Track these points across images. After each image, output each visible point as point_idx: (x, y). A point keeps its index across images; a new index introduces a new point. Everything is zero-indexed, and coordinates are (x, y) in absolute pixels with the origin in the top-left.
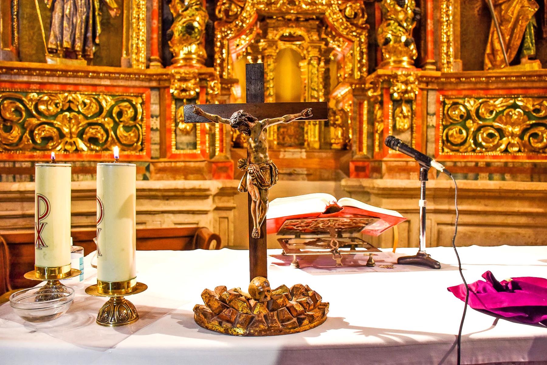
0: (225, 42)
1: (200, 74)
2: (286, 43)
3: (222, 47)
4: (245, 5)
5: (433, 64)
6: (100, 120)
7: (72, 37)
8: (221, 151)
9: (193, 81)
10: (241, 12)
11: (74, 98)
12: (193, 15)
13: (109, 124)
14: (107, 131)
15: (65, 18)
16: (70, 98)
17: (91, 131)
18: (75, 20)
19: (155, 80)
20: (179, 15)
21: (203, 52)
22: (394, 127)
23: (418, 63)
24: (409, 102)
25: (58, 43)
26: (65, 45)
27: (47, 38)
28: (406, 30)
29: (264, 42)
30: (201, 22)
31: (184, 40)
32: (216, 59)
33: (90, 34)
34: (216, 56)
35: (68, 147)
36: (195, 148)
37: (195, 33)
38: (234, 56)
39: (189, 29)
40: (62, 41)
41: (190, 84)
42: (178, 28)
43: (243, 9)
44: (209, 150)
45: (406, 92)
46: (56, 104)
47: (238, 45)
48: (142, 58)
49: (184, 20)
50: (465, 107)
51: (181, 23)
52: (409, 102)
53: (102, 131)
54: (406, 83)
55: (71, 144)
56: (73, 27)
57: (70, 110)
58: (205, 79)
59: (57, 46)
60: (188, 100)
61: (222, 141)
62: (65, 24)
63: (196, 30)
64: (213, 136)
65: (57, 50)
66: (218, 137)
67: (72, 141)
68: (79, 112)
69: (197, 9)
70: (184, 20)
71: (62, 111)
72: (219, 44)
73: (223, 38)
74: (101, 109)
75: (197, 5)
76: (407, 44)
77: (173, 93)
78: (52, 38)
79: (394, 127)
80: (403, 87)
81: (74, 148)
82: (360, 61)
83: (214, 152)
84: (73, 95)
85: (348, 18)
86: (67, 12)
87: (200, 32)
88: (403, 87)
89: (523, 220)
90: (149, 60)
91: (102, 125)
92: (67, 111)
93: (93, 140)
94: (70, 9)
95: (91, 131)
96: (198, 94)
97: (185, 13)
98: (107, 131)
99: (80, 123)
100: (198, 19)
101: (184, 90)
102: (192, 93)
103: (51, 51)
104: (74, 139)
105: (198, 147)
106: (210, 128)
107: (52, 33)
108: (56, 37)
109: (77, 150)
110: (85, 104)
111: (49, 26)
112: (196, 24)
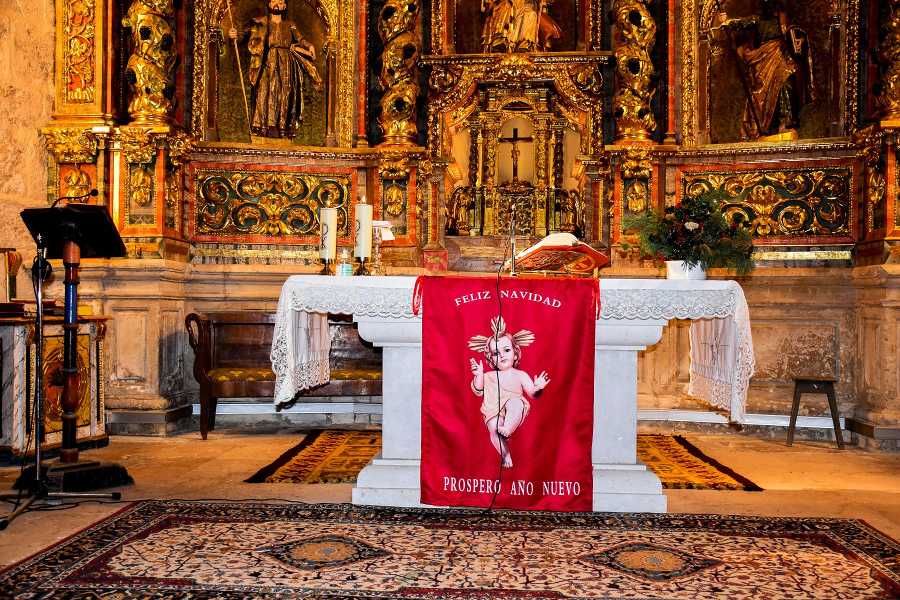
0: (439, 116)
1: (410, 153)
2: (515, 112)
3: (436, 121)
4: (461, 73)
5: (673, 136)
6: (305, 201)
7: (277, 114)
8: (434, 239)
9: (402, 161)
10: (457, 82)
11: (278, 179)
12: (403, 89)
13: (313, 206)
14: (311, 213)
15: (271, 96)
16: (274, 178)
17: (296, 213)
18: (280, 98)
19: (363, 159)
20: (388, 89)
21: (414, 128)
22: (626, 208)
23: (657, 136)
24: (644, 180)
25: (263, 121)
26: (270, 123)
27: (252, 116)
28: (642, 99)
29: (484, 115)
30: (411, 96)
31: (394, 117)
32: (428, 136)
33: (294, 111)
34: (429, 132)
35: (271, 229)
36: (405, 233)
37: (406, 109)
38: (452, 129)
39: (400, 103)
40: (266, 119)
41: (399, 165)
42: (388, 102)
43: (459, 78)
44: (420, 237)
45: (638, 169)
46: (260, 185)
47: (455, 118)
48: (349, 136)
49: (393, 95)
50: (709, 185)
51: (390, 98)
52: (644, 180)
53: (307, 214)
54: (637, 159)
55: (274, 226)
56: (278, 104)
57: (274, 191)
58: (416, 159)
59: (262, 125)
60: (396, 181)
61: (434, 227)
62: (270, 102)
63: (407, 106)
64: (426, 220)
65: (260, 129)
66: (430, 223)
67: (275, 224)
68: (283, 193)
69: (407, 82)
70: (393, 95)
71: (266, 192)
72: (431, 118)
73: (437, 111)
74: (306, 190)
75: (407, 77)
76: (641, 114)
77: (381, 173)
78: (256, 118)
79: (626, 208)
80: (634, 164)
81: (277, 230)
82: (594, 135)
83: (427, 240)
84: (278, 176)
85: (577, 84)
86: (273, 89)
87: (411, 107)
88: (634, 164)
89: (776, 313)
90: (356, 138)
91: (307, 207)
92: (271, 192)
93: (297, 223)
94: (275, 86)
95: (296, 213)
96: (408, 174)
97: (394, 86)
98: (311, 213)
99: (283, 204)
100: (408, 93)
101: (393, 171)
102: (402, 173)
103: (254, 130)
104: (277, 222)
105: (409, 231)
106: (420, 211)
107: (257, 111)
108: (260, 116)
109: (280, 233)
110: (289, 185)
111: (253, 104)
112: (406, 99)
